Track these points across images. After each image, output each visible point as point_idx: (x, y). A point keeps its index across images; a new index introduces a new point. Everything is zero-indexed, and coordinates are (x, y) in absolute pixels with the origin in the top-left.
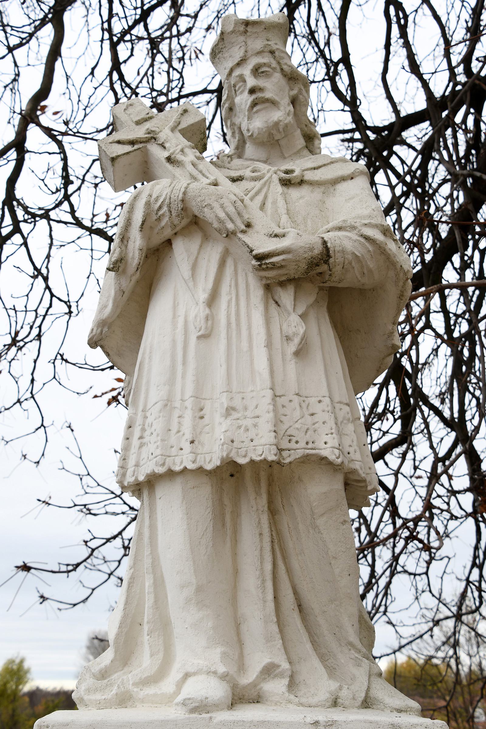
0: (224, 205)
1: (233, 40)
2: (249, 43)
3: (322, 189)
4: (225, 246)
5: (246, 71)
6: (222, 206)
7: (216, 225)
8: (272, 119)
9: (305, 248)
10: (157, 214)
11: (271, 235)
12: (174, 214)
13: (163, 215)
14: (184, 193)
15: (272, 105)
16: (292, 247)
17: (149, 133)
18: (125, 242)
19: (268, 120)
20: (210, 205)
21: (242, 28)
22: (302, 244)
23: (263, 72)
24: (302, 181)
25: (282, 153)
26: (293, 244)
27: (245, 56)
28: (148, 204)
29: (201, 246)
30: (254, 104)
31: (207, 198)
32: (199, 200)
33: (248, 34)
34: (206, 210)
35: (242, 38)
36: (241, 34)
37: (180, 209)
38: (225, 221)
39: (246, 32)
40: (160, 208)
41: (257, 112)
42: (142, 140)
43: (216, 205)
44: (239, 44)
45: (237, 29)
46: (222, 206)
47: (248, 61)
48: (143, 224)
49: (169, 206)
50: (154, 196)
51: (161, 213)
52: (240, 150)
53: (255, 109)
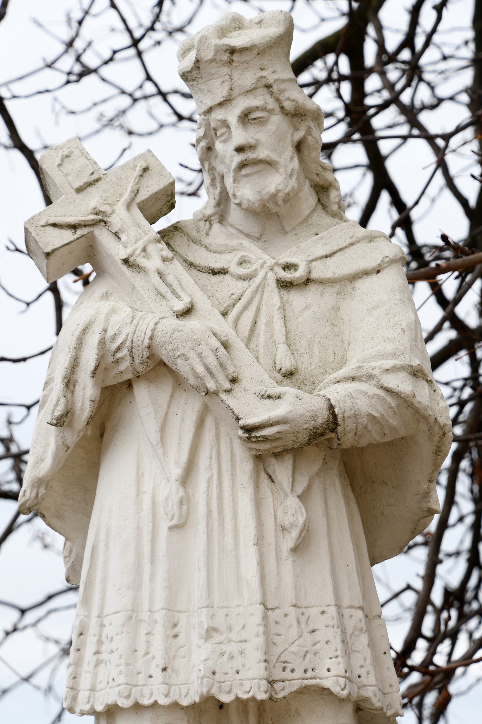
0: (203, 355)
1: (213, 71)
2: (235, 77)
3: (337, 288)
4: (204, 401)
5: (232, 115)
6: (200, 356)
7: (192, 381)
8: (267, 190)
9: (306, 416)
10: (114, 355)
13: (122, 358)
14: (151, 338)
15: (269, 166)
16: (289, 415)
17: (96, 214)
18: (71, 387)
19: (262, 189)
20: (184, 355)
21: (225, 57)
22: (302, 412)
23: (255, 119)
24: (308, 279)
25: (282, 226)
26: (290, 412)
27: (230, 95)
28: (102, 342)
29: (172, 397)
30: (243, 165)
31: (180, 346)
32: (170, 348)
33: (234, 64)
34: (179, 361)
35: (226, 70)
36: (224, 65)
37: (145, 356)
38: (204, 378)
39: (231, 62)
40: (118, 349)
41: (246, 176)
42: (86, 223)
43: (192, 355)
44: (220, 77)
45: (218, 57)
46: (200, 356)
47: (235, 102)
48: (95, 369)
50: (110, 333)
51: (119, 355)
52: (222, 207)
53: (244, 172)
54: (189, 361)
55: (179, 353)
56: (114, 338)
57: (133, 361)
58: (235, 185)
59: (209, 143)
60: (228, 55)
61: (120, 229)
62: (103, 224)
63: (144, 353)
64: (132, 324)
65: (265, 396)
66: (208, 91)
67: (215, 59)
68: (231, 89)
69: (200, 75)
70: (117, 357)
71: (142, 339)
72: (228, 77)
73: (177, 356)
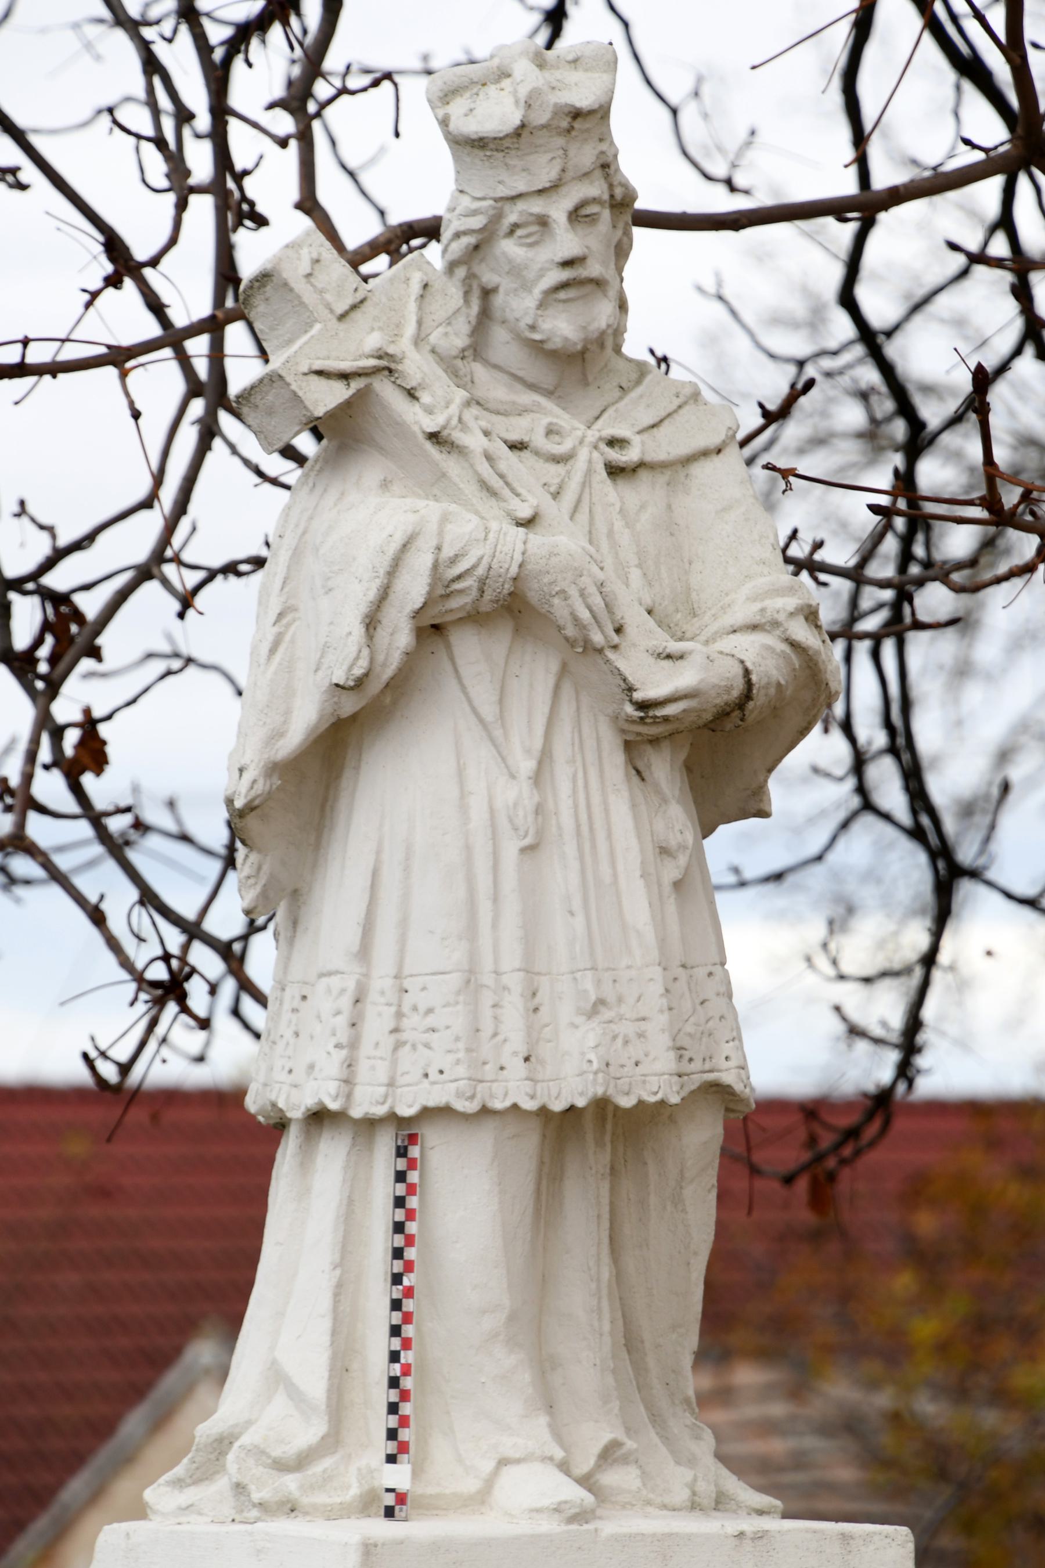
0: (586, 592)
2: (572, 153)
6: (582, 593)
9: (720, 687)
11: (659, 655)
12: (488, 596)
13: (461, 592)
17: (380, 357)
20: (563, 591)
22: (715, 681)
26: (702, 680)
27: (560, 179)
32: (546, 580)
33: (573, 133)
35: (560, 141)
36: (559, 134)
37: (506, 592)
38: (590, 627)
39: (570, 130)
40: (459, 577)
47: (564, 190)
49: (483, 582)
53: (562, 295)
54: (569, 602)
55: (558, 589)
56: (453, 561)
57: (482, 596)
58: (539, 312)
59: (482, 239)
60: (569, 119)
61: (420, 385)
62: (386, 373)
63: (506, 586)
64: (488, 542)
65: (664, 655)
66: (524, 170)
67: (550, 125)
68: (563, 171)
69: (516, 146)
70: (451, 589)
71: (507, 566)
72: (561, 152)
73: (554, 593)
